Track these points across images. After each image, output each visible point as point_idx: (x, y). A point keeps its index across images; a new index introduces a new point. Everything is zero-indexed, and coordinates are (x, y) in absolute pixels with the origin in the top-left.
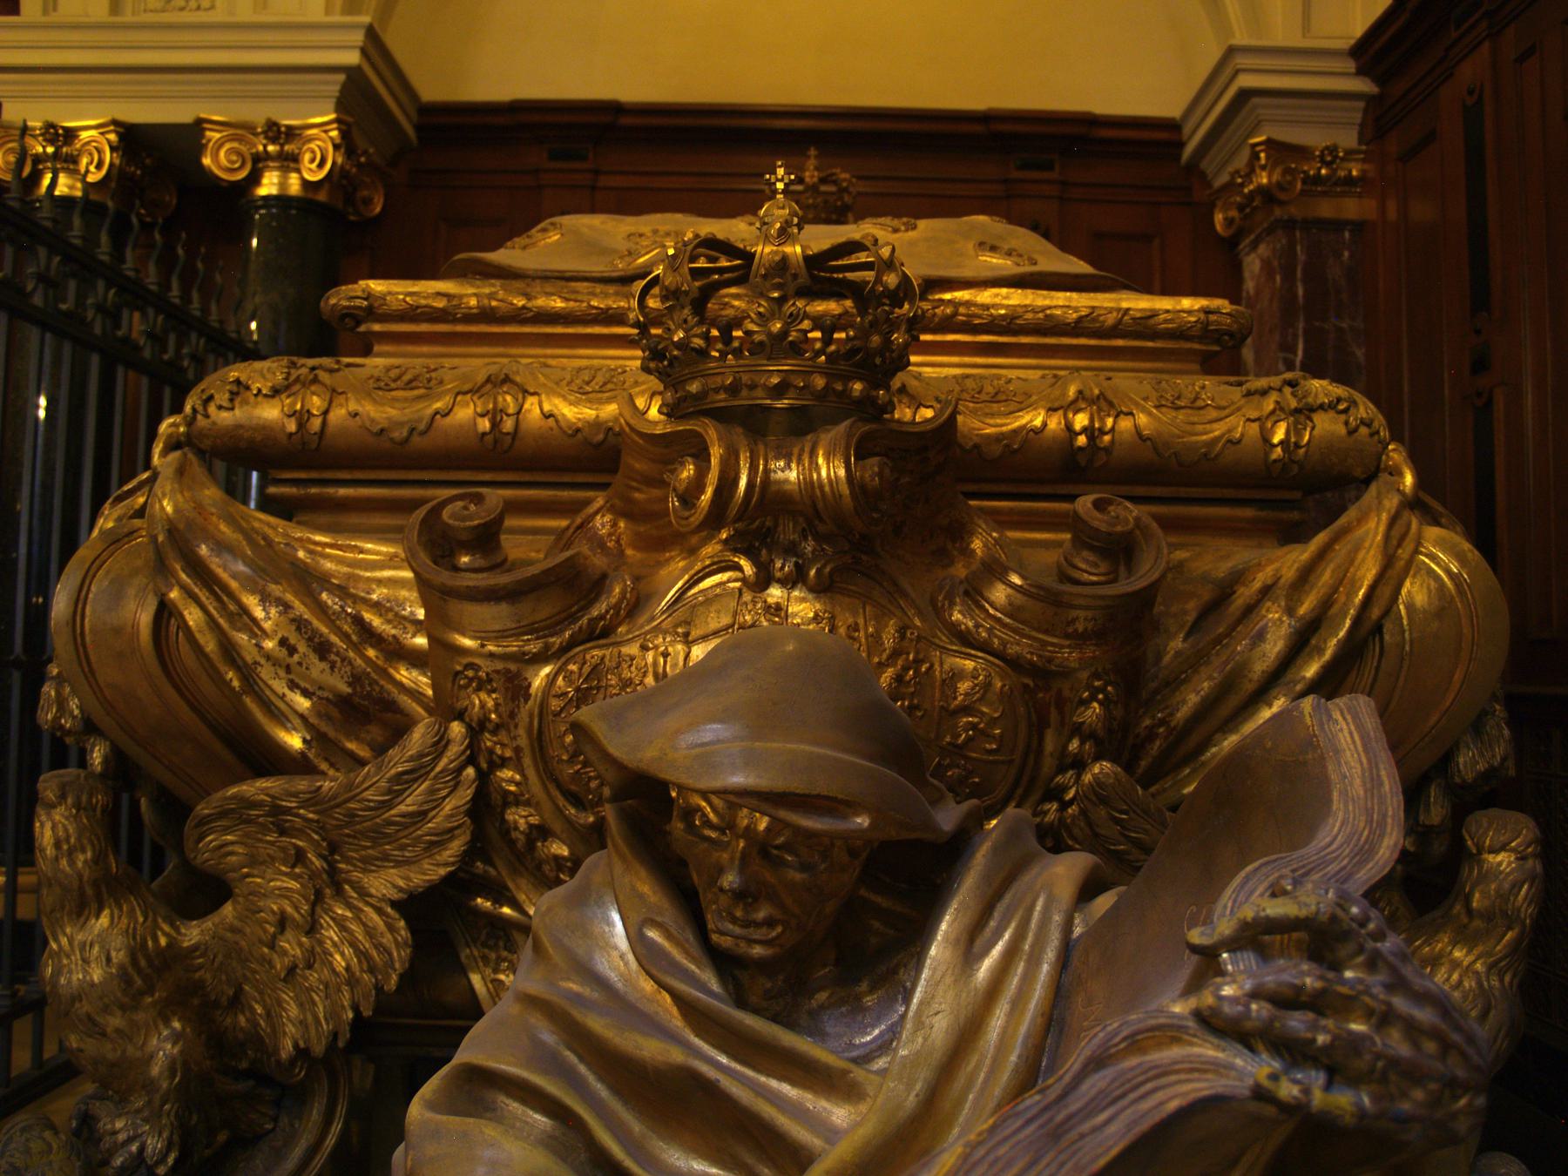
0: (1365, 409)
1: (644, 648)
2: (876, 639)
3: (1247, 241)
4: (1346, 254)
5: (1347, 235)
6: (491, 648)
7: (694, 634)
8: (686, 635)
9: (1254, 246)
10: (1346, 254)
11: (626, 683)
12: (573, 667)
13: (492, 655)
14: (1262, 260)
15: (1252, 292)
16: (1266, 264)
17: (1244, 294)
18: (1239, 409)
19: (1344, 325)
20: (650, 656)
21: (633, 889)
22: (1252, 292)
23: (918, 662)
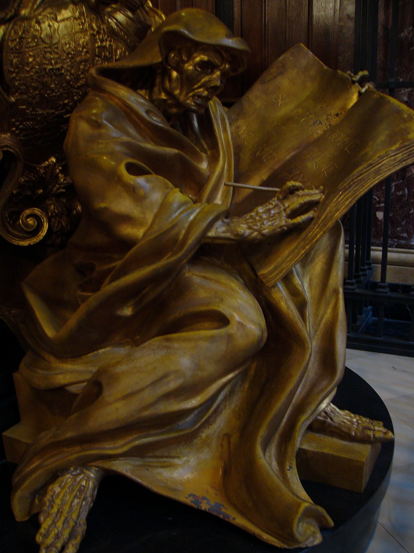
7: (59, 18)
8: (56, 18)
12: (16, 27)
21: (138, 101)
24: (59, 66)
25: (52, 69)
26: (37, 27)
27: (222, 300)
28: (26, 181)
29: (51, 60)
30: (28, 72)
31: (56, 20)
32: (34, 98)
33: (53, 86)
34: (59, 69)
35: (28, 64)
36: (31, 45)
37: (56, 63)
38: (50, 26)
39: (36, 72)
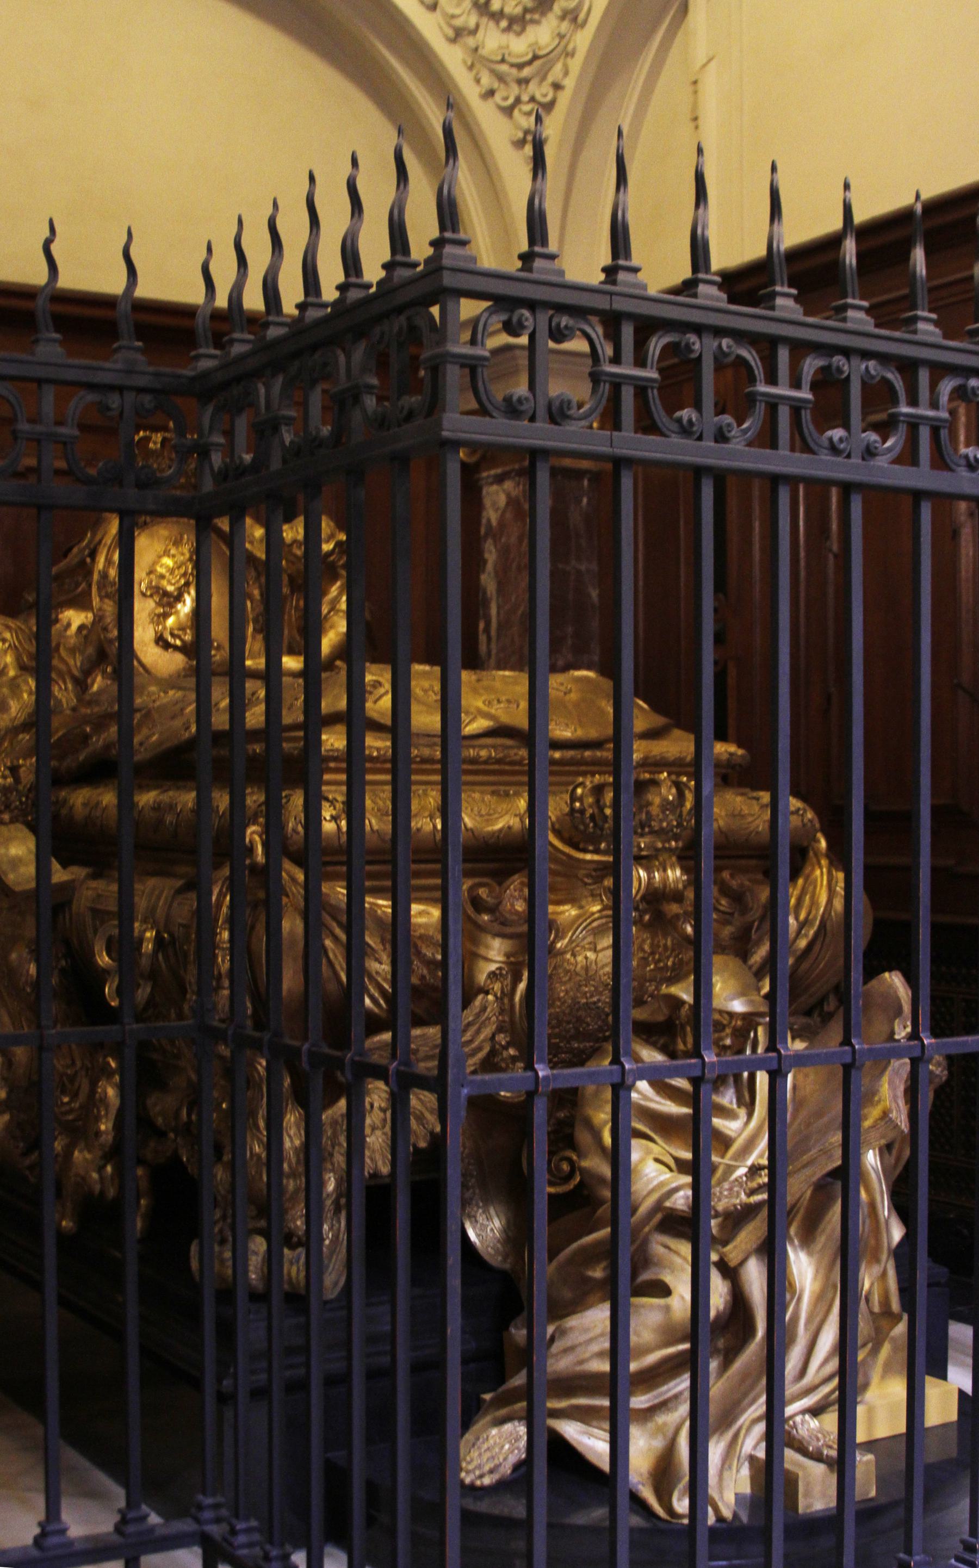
0: (810, 815)
1: (574, 955)
2: (665, 945)
3: (493, 472)
4: (585, 500)
5: (586, 483)
6: (512, 959)
7: (599, 947)
8: (595, 948)
9: (500, 479)
10: (585, 500)
11: (567, 971)
13: (511, 963)
14: (508, 496)
15: (494, 522)
16: (512, 502)
17: (484, 521)
18: (759, 816)
19: (583, 568)
20: (580, 958)
22: (494, 522)
23: (679, 954)
24: (595, 999)
25: (587, 1003)
26: (572, 960)
27: (673, 1272)
28: (566, 1117)
29: (586, 993)
30: (559, 1007)
31: (595, 950)
32: (568, 1031)
33: (589, 1019)
34: (595, 1003)
35: (559, 999)
36: (564, 979)
37: (592, 996)
38: (586, 958)
39: (569, 1006)
